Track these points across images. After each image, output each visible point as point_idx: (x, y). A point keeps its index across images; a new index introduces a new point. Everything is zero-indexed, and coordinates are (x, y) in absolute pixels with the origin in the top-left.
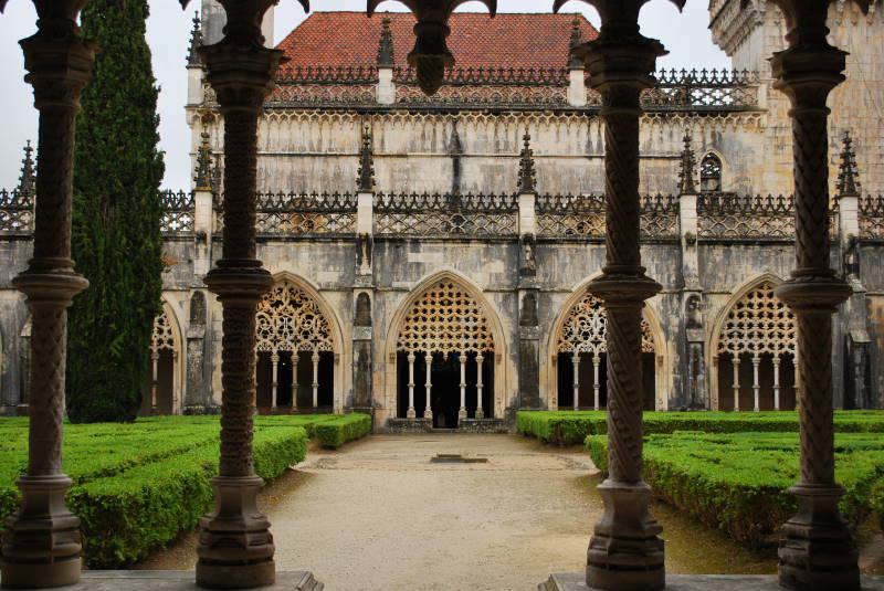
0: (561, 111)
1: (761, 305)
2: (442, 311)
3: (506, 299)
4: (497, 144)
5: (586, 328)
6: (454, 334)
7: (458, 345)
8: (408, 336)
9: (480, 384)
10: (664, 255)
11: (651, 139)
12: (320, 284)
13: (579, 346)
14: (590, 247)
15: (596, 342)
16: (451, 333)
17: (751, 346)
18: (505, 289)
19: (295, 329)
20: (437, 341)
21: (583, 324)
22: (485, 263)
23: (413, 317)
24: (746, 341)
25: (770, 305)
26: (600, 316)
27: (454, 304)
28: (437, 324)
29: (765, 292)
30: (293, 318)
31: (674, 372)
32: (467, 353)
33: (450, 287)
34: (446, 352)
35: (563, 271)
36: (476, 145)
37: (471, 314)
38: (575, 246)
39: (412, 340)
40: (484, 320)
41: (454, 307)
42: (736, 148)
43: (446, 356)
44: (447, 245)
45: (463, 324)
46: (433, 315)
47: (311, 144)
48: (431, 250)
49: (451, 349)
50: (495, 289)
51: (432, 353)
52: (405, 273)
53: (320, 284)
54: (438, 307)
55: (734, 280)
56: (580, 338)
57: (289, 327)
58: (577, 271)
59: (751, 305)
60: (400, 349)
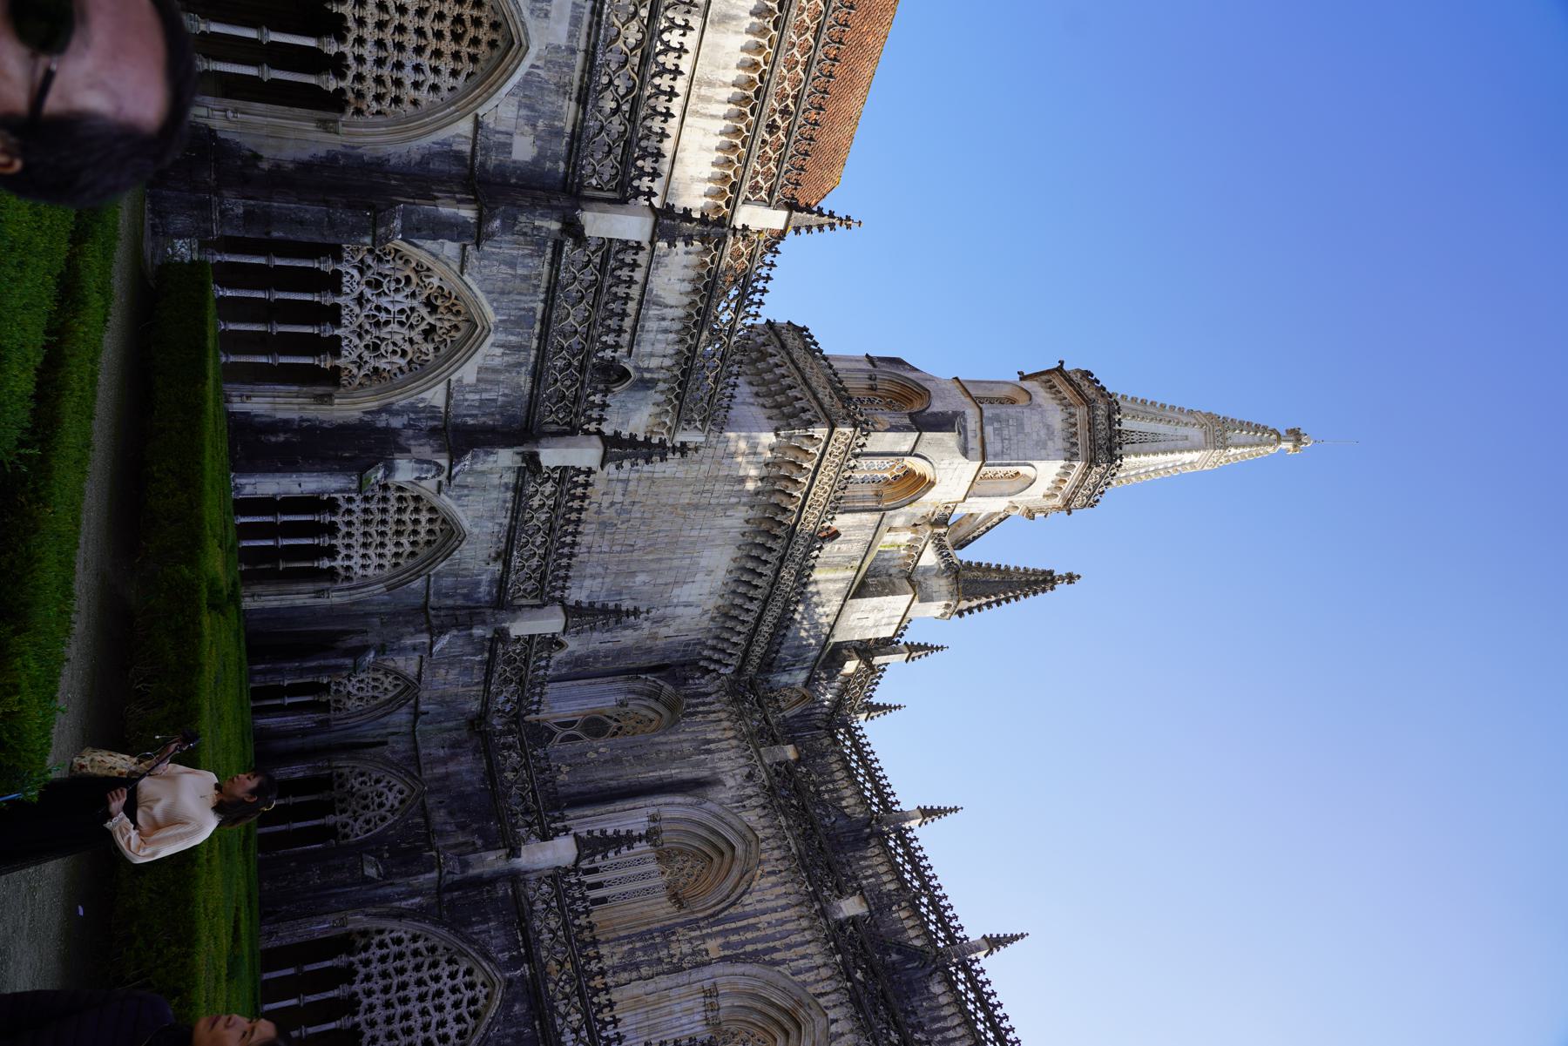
1: (416, 522)
3: (458, 156)
4: (710, 84)
7: (360, 41)
10: (511, 411)
11: (666, 306)
13: (355, 273)
14: (540, 306)
15: (360, 300)
16: (390, 29)
17: (349, 512)
18: (479, 158)
21: (398, 281)
22: (534, 126)
25: (415, 532)
26: (412, 309)
27: (454, 47)
29: (436, 527)
31: (302, 420)
32: (341, 56)
33: (492, 44)
35: (505, 262)
38: (544, 284)
40: (415, 103)
41: (447, 46)
42: (630, 405)
44: (580, 57)
45: (409, 59)
48: (575, 21)
49: (351, 24)
55: (459, 498)
58: (501, 284)
59: (417, 510)
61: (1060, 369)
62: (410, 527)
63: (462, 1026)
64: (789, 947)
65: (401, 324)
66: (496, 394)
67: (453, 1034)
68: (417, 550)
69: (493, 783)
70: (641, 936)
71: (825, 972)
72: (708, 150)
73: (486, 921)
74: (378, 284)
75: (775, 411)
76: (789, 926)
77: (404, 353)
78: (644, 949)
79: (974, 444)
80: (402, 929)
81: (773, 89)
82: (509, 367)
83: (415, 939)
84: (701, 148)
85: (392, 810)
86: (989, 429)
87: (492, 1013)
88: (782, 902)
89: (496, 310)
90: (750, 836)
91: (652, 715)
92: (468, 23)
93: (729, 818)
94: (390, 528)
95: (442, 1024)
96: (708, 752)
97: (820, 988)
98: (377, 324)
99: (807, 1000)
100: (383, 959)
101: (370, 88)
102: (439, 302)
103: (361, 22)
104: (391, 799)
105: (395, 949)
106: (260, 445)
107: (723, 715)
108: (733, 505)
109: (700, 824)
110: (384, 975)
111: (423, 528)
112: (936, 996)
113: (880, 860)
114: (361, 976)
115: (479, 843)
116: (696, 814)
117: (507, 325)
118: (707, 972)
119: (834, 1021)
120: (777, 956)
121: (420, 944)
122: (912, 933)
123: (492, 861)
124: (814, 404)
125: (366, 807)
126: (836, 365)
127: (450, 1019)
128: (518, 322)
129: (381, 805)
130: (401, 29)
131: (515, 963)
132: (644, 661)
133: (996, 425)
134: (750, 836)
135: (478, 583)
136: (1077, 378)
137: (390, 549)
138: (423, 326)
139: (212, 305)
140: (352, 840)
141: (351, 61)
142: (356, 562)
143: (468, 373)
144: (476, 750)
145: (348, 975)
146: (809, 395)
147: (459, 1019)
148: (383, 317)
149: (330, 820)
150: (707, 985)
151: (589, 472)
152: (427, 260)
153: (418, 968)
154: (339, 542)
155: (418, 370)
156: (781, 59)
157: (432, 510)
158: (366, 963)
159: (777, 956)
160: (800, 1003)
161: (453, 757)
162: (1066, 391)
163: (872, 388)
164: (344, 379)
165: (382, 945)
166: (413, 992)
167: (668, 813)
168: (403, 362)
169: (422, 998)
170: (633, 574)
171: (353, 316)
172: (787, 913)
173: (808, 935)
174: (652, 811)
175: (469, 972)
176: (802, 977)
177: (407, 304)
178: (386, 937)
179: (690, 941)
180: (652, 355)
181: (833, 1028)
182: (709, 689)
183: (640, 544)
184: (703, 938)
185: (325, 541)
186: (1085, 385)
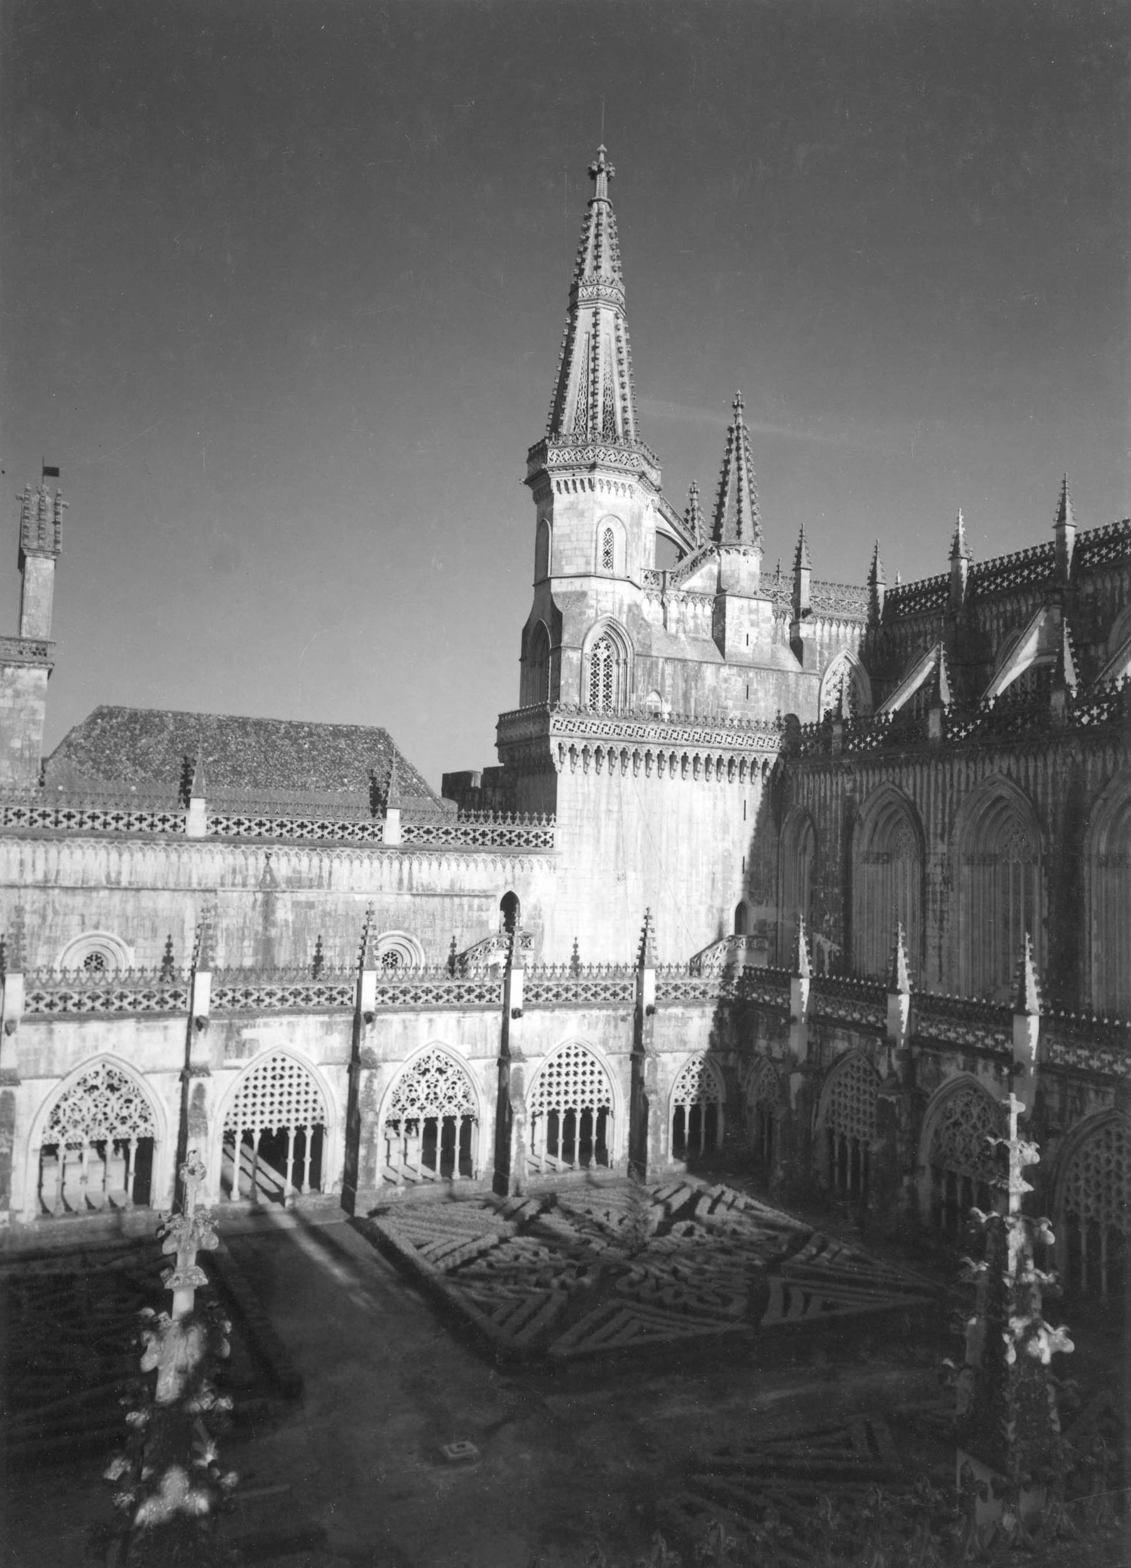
5: (413, 1095)
8: (236, 1115)
9: (308, 1160)
12: (143, 1066)
17: (558, 1103)
19: (112, 1116)
24: (554, 1098)
30: (110, 1104)
32: (297, 1128)
34: (275, 1127)
39: (240, 1119)
41: (286, 1081)
43: (274, 1133)
47: (108, 876)
49: (281, 1125)
51: (262, 1131)
53: (143, 1066)
54: (269, 1082)
56: (408, 1105)
57: (105, 1114)
60: (227, 1128)
65: (436, 1086)
68: (588, 1062)
74: (413, 1100)
78: (935, 902)
83: (833, 1092)
97: (980, 773)
102: (422, 1069)
103: (280, 1121)
113: (987, 610)
116: (868, 825)
119: (1001, 771)
133: (563, 563)
145: (843, 1137)
148: (432, 1096)
152: (399, 1078)
166: (855, 1105)
167: (864, 848)
168: (459, 1083)
177: (424, 1084)
181: (1005, 772)
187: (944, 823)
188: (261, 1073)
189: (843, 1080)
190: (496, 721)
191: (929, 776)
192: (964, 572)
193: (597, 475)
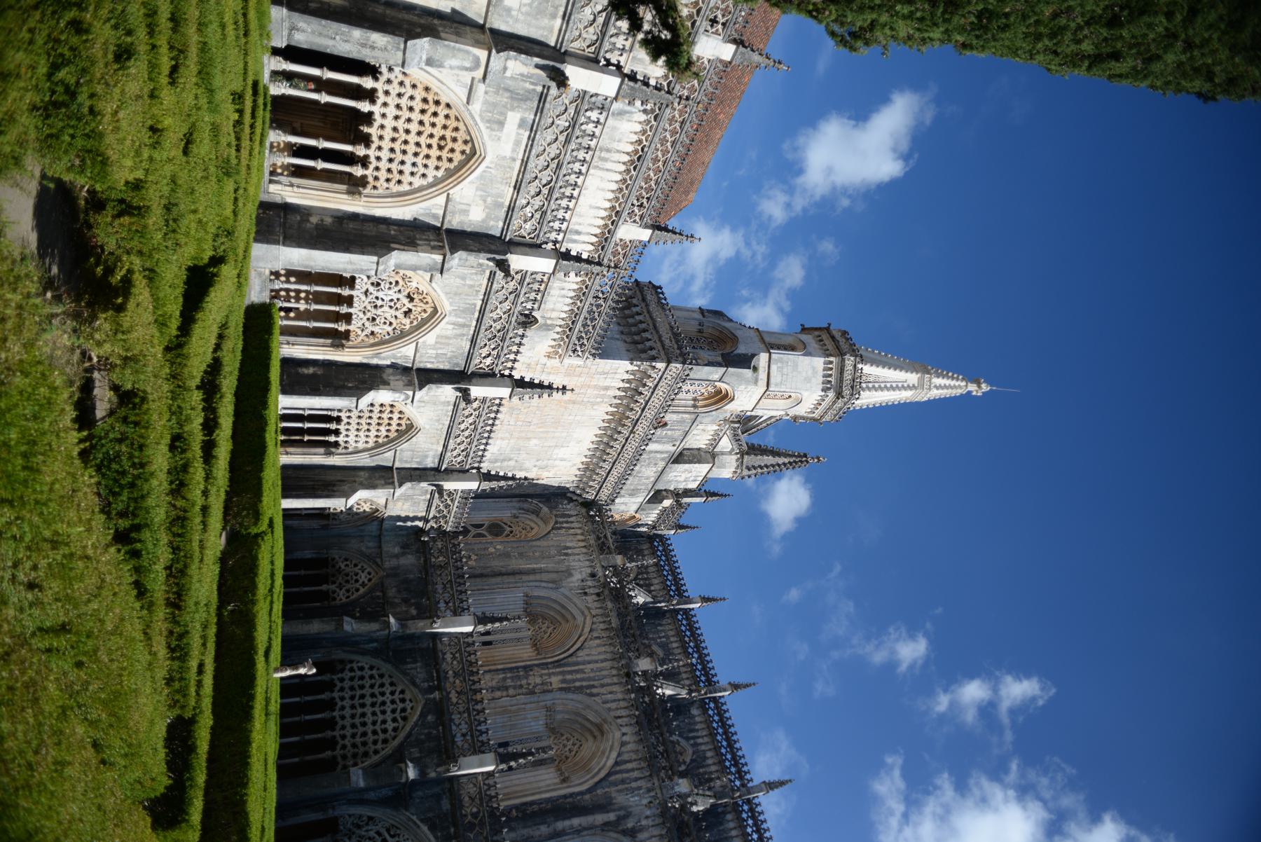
0: (615, 217)
2: (431, 136)
4: (608, 150)
6: (397, 146)
7: (380, 148)
8: (401, 84)
9: (321, 165)
15: (366, 293)
18: (448, 218)
20: (390, 123)
22: (485, 201)
23: (430, 99)
27: (438, 153)
28: (414, 127)
32: (367, 157)
34: (373, 131)
36: (614, 128)
37: (422, 170)
38: (483, 291)
41: (434, 152)
43: (366, 129)
44: (518, 163)
45: (409, 159)
46: (427, 124)
48: (517, 143)
49: (375, 138)
50: (450, 207)
51: (371, 114)
52: (495, 105)
60: (384, 69)
61: (828, 329)
62: (387, 421)
63: (396, 725)
64: (602, 686)
66: (447, 351)
67: (390, 728)
69: (427, 574)
70: (511, 669)
71: (623, 704)
72: (603, 190)
73: (415, 662)
74: (378, 284)
75: (632, 347)
76: (604, 673)
77: (391, 324)
78: (512, 678)
79: (762, 375)
80: (365, 661)
81: (649, 156)
82: (456, 336)
83: (371, 668)
84: (598, 188)
85: (363, 585)
86: (773, 367)
87: (415, 718)
88: (602, 657)
89: (451, 304)
90: (586, 612)
91: (533, 525)
92: (449, 139)
93: (575, 600)
94: (374, 421)
95: (384, 722)
96: (566, 554)
97: (618, 713)
98: (376, 307)
99: (609, 720)
100: (352, 679)
101: (383, 175)
103: (381, 138)
104: (363, 577)
105: (359, 673)
106: (300, 377)
107: (579, 531)
108: (598, 403)
109: (555, 601)
110: (352, 688)
111: (394, 422)
112: (694, 716)
114: (337, 688)
115: (414, 612)
116: (553, 595)
117: (456, 312)
118: (549, 696)
119: (624, 734)
120: (594, 691)
121: (374, 672)
122: (684, 676)
123: (420, 626)
124: (659, 344)
125: (347, 582)
126: (677, 313)
127: (389, 719)
128: (464, 311)
129: (357, 581)
130: (406, 142)
131: (431, 690)
132: (531, 491)
134: (586, 612)
135: (426, 456)
136: (838, 335)
137: (373, 433)
138: (405, 309)
139: (277, 331)
140: (338, 602)
141: (372, 159)
142: (351, 439)
143: (430, 338)
144: (417, 551)
146: (656, 337)
147: (394, 720)
148: (379, 303)
149: (324, 587)
150: (549, 703)
151: (501, 399)
153: (372, 686)
154: (342, 427)
155: (400, 336)
156: (656, 139)
157: (401, 412)
158: (342, 680)
159: (594, 691)
160: (605, 721)
161: (404, 554)
162: (828, 342)
163: (700, 331)
164: (352, 335)
165: (352, 670)
166: (368, 700)
167: (536, 593)
169: (373, 705)
170: (529, 439)
171: (360, 302)
172: (604, 664)
173: (615, 680)
174: (526, 589)
175: (402, 692)
176: (608, 705)
177: (395, 297)
178: (355, 666)
179: (541, 676)
180: (553, 310)
181: (625, 738)
182: (572, 513)
183: (535, 421)
184: (549, 675)
185: (333, 426)
186: (842, 341)
187: (574, 681)
188: (452, 123)
189: (386, 680)
190: (657, 284)
191: (606, 660)
192: (691, 606)
193: (831, 394)
